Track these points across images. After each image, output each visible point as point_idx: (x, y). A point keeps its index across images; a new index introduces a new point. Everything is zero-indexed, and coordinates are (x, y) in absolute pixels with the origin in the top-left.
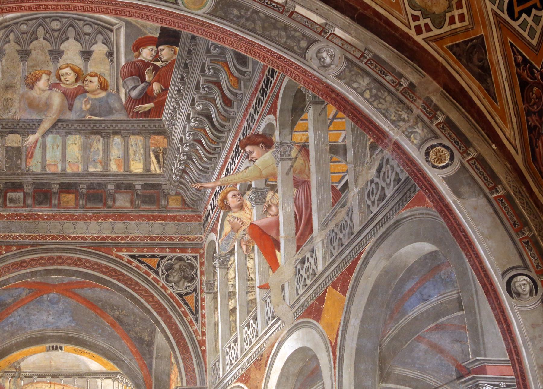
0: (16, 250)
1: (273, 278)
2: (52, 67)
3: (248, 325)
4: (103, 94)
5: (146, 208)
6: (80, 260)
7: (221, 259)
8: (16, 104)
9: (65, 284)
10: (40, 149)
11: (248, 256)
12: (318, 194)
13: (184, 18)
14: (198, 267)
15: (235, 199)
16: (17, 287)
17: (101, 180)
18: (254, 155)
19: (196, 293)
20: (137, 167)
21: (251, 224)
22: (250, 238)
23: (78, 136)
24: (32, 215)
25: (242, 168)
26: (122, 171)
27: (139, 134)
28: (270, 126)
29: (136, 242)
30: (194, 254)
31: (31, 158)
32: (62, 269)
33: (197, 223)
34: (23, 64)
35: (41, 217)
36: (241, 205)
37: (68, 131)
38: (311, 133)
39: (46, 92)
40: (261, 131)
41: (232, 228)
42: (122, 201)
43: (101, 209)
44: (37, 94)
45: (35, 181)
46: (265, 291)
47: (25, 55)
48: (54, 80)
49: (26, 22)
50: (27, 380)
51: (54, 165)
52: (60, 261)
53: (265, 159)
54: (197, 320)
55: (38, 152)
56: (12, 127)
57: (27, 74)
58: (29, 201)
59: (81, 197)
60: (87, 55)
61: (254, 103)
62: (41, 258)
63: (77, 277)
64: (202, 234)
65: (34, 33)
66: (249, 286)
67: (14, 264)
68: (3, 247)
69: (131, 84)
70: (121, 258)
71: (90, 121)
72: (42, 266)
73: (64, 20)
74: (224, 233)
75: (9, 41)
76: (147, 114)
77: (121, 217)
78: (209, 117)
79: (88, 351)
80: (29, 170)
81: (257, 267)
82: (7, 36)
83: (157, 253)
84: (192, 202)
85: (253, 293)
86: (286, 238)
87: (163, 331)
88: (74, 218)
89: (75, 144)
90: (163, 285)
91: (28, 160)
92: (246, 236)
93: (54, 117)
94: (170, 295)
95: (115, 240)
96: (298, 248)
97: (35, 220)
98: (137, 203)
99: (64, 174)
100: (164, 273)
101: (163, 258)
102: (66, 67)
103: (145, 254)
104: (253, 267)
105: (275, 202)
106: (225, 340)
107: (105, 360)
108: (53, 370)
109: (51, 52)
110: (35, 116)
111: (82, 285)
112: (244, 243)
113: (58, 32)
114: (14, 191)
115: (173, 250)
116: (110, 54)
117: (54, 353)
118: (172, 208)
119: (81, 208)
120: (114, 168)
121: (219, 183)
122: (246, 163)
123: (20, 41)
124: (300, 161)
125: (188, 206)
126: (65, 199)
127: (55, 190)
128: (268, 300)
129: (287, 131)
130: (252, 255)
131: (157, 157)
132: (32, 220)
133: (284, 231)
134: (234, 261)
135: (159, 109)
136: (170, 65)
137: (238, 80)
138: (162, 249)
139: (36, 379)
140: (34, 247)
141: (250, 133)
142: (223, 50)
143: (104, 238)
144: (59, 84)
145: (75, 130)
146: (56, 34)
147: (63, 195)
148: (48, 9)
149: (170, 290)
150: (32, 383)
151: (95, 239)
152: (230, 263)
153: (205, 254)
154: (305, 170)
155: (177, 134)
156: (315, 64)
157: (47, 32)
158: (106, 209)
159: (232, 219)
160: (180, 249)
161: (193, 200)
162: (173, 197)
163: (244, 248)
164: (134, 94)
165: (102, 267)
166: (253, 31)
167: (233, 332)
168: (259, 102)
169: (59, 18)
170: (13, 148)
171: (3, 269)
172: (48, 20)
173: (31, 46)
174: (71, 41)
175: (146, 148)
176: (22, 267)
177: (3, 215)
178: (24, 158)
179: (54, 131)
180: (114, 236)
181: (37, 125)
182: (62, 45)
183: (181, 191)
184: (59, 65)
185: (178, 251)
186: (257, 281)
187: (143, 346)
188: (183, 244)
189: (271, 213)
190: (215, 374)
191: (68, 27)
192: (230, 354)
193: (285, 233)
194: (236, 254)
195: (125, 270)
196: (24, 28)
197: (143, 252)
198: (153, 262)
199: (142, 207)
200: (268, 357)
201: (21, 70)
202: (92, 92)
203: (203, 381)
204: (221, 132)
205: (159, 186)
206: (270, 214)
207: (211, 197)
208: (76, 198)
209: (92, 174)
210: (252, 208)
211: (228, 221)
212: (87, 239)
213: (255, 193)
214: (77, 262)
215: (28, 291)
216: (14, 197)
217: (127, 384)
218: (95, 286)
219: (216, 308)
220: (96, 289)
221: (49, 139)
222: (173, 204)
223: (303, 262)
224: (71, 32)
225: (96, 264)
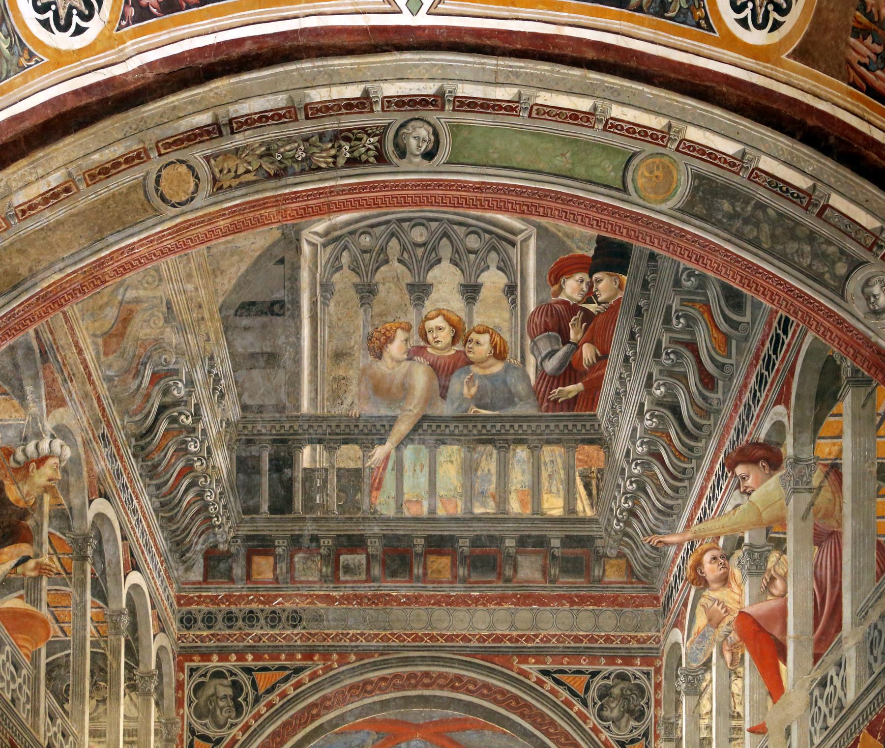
0: (356, 661)
1: (774, 715)
2: (412, 317)
4: (497, 367)
5: (568, 583)
6: (459, 678)
7: (690, 678)
8: (354, 388)
9: (436, 723)
10: (394, 473)
11: (733, 673)
12: (854, 556)
13: (636, 218)
14: (652, 692)
15: (716, 565)
16: (357, 729)
17: (494, 530)
18: (749, 482)
19: (647, 739)
20: (553, 505)
21: (740, 612)
22: (737, 638)
23: (455, 447)
24: (381, 595)
25: (729, 508)
26: (528, 512)
27: (558, 442)
28: (778, 427)
29: (551, 645)
30: (645, 668)
31: (378, 489)
32: (430, 696)
33: (651, 609)
34: (365, 311)
35: (396, 599)
36: (724, 577)
37: (441, 437)
38: (847, 441)
39: (403, 364)
40: (762, 436)
41: (710, 620)
42: (529, 569)
43: (494, 585)
44: (387, 367)
45: (385, 532)
47: (367, 293)
48: (416, 340)
49: (370, 230)
51: (417, 502)
52: (426, 681)
53: (767, 489)
55: (389, 478)
56: (347, 431)
57: (370, 329)
58: (376, 571)
59: (461, 562)
60: (471, 292)
61: (752, 382)
62: (396, 676)
63: (455, 710)
64: (658, 631)
65: (383, 250)
66: (734, 728)
67: (352, 687)
68: (335, 656)
69: (545, 347)
70: (526, 674)
71: (476, 418)
72: (399, 690)
73: (434, 225)
75: (341, 267)
76: (571, 403)
77: (526, 600)
78: (675, 410)
80: (375, 512)
81: (747, 692)
82: (338, 258)
83: (584, 666)
84: (644, 571)
85: (739, 741)
86: (797, 639)
88: (451, 602)
89: (452, 462)
90: (594, 724)
91: (374, 493)
92: (731, 635)
93: (415, 411)
95: (517, 641)
96: (817, 657)
97: (385, 605)
98: (553, 572)
99: (432, 519)
100: (595, 703)
101: (594, 674)
102: (437, 316)
103: (565, 667)
104: (741, 693)
105: (781, 572)
109: (411, 287)
110: (384, 411)
111: (462, 725)
112: (727, 648)
113: (422, 249)
114: (352, 552)
115: (611, 660)
116: (510, 290)
118: (610, 583)
119: (460, 582)
120: (515, 507)
121: (689, 535)
122: (736, 497)
123: (359, 267)
124: (826, 494)
125: (638, 578)
126: (435, 566)
127: (419, 549)
129: (806, 436)
130: (740, 669)
131: (587, 486)
132: (381, 606)
133: (795, 625)
134: (711, 681)
135: (590, 397)
136: (612, 310)
137: (727, 338)
138: (594, 659)
140: (385, 656)
141: (744, 439)
142: (702, 278)
143: (498, 639)
144: (425, 348)
145: (451, 435)
146: (420, 251)
147: (431, 558)
148: (406, 204)
149: (605, 734)
151: (485, 641)
152: (704, 684)
153: (664, 667)
154: (833, 512)
155: (621, 443)
156: (859, 307)
157: (404, 248)
158: (501, 584)
159: (710, 603)
160: (622, 658)
161: (645, 567)
162: (613, 562)
163: (728, 656)
164: (551, 365)
165: (495, 692)
166: (755, 243)
168: (761, 380)
169: (425, 222)
170: (348, 470)
171: (335, 697)
172: (406, 225)
173: (378, 276)
174: (445, 264)
175: (569, 469)
176: (366, 692)
177: (334, 597)
178: (366, 488)
179: (417, 437)
180: (515, 633)
181: (387, 428)
182: (430, 274)
183: (627, 551)
184: (424, 312)
185: (620, 661)
186: (747, 718)
188: (627, 649)
189: (775, 592)
191: (441, 239)
193: (796, 630)
194: (714, 668)
195: (533, 698)
196: (366, 240)
197: (562, 664)
199: (562, 580)
201: (361, 323)
202: (480, 363)
204: (696, 439)
205: (591, 539)
206: (772, 595)
207: (676, 563)
208: (454, 564)
209: (479, 519)
210: (743, 582)
211: (703, 606)
212: (470, 641)
213: (749, 554)
214: (455, 683)
215: (376, 737)
216: (350, 562)
218: (485, 727)
220: (486, 732)
221: (408, 452)
222: (613, 575)
223: (823, 684)
224: (445, 249)
225: (486, 686)
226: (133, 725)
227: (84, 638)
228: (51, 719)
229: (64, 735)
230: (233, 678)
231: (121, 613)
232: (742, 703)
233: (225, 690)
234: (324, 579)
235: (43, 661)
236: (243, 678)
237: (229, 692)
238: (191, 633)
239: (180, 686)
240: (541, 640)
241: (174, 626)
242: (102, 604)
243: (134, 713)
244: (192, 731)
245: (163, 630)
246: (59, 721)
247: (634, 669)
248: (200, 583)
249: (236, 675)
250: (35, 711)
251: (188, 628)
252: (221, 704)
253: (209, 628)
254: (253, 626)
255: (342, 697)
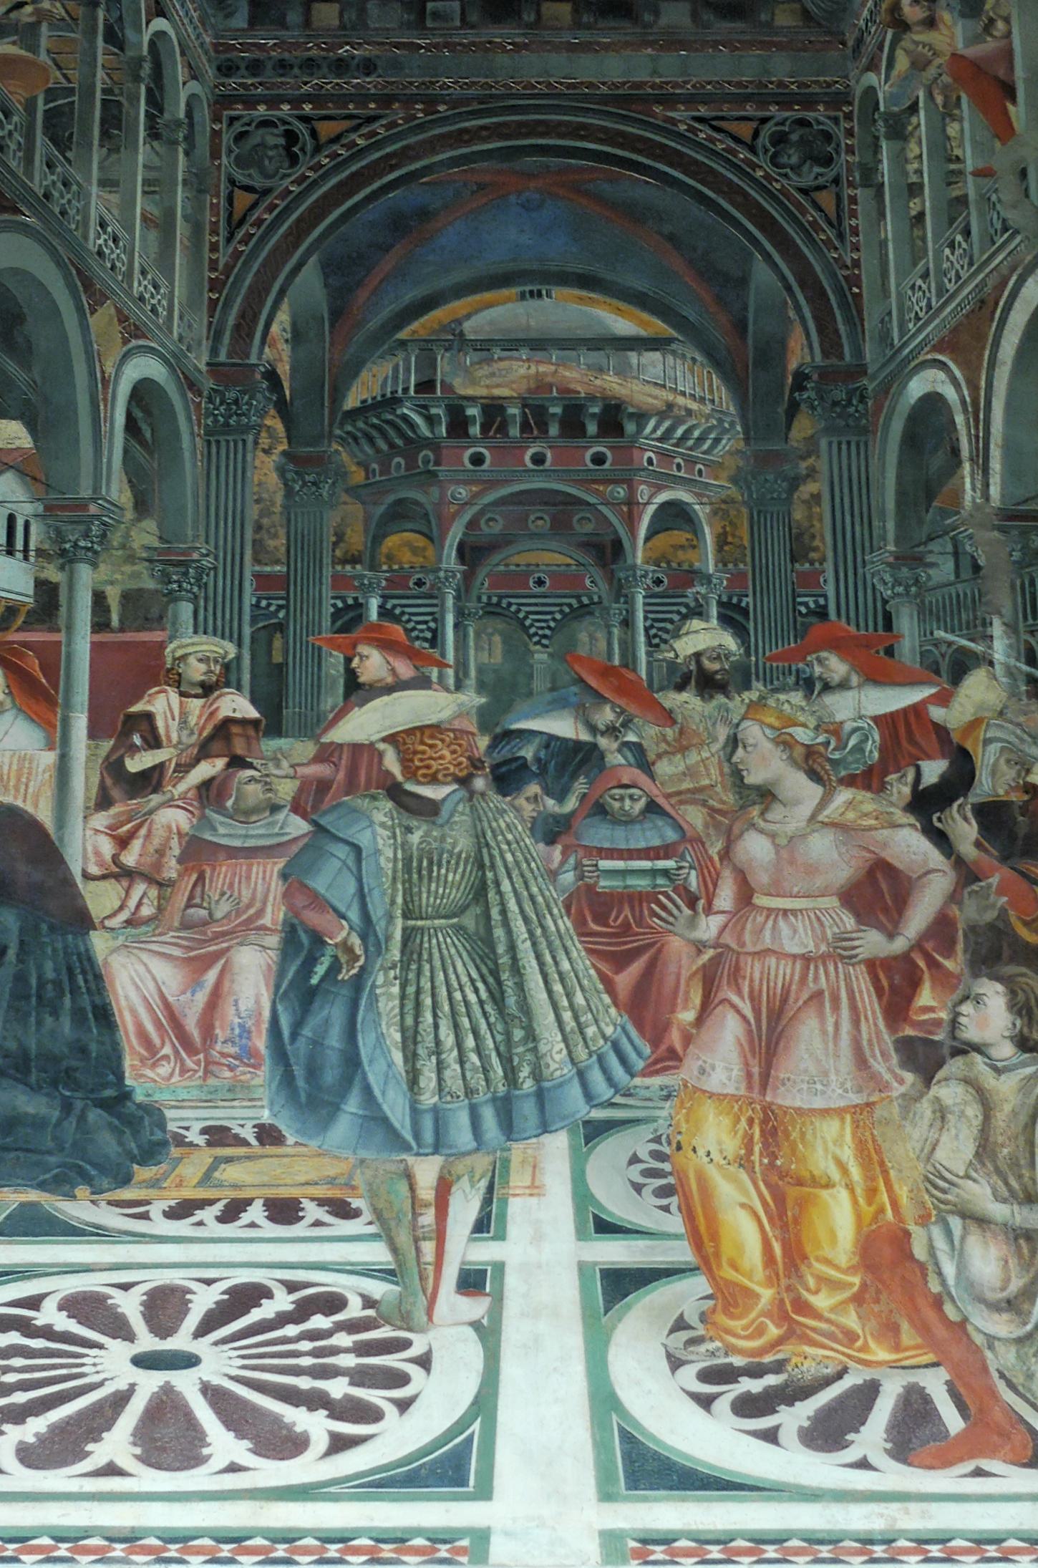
1: (1003, 158)
3: (952, 246)
11: (949, 112)
21: (953, 55)
46: (987, 182)
50: (477, 356)
54: (841, 236)
58: (474, 17)
66: (952, 172)
70: (673, 121)
72: (506, 139)
74: (894, 73)
77: (672, 42)
79: (608, 300)
83: (750, 110)
87: (767, 257)
94: (783, 191)
101: (764, 121)
104: (958, 136)
105: (1004, 13)
106: (902, 274)
107: (645, 316)
108: (533, 335)
117: (533, 303)
128: (994, 198)
130: (956, 112)
134: (919, 125)
139: (497, 353)
140: (486, 103)
150: (489, 361)
151: (618, 88)
159: (912, 47)
163: (939, 99)
167: (921, 259)
186: (969, 162)
187: (728, 284)
189: (995, 33)
190: (885, 337)
192: (914, 300)
198: (745, 130)
200: (997, 304)
203: (858, 352)
210: (955, 24)
217: (694, 359)
219: (882, 215)
226: (153, 175)
227: (93, 85)
228: (49, 166)
229: (65, 185)
230: (287, 127)
231: (141, 60)
232: (961, 145)
233: (274, 139)
234: (408, 26)
235: (41, 107)
236: (300, 127)
237: (282, 141)
238: (232, 82)
239: (216, 134)
240: (694, 86)
241: (210, 72)
242: (116, 50)
243: (157, 162)
244: (232, 182)
245: (194, 77)
246: (59, 169)
247: (819, 114)
248: (243, 30)
249: (289, 123)
250: (29, 160)
251: (227, 76)
252: (270, 153)
253: (254, 75)
254: (312, 74)
255: (432, 146)
